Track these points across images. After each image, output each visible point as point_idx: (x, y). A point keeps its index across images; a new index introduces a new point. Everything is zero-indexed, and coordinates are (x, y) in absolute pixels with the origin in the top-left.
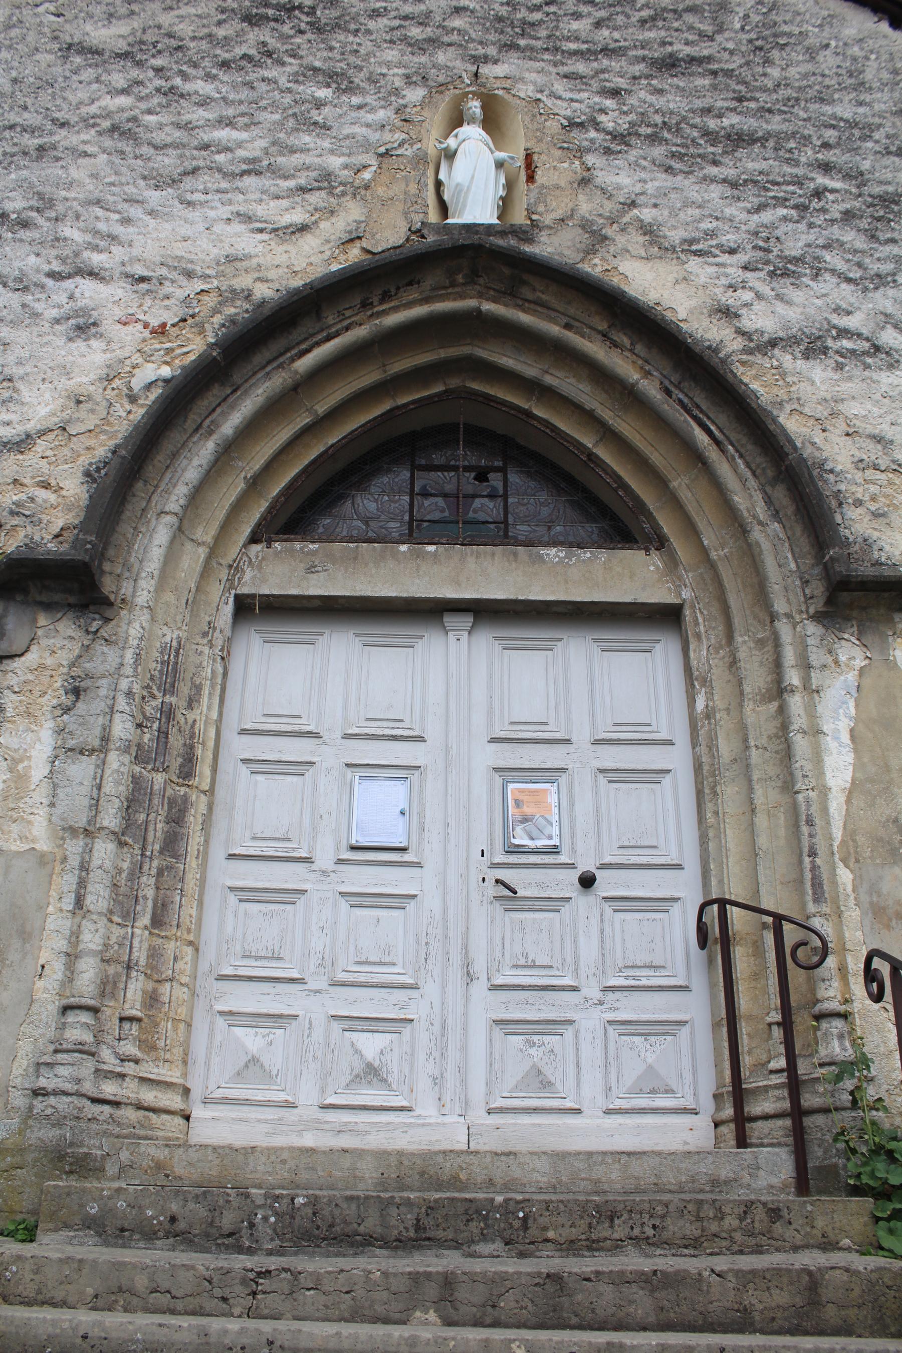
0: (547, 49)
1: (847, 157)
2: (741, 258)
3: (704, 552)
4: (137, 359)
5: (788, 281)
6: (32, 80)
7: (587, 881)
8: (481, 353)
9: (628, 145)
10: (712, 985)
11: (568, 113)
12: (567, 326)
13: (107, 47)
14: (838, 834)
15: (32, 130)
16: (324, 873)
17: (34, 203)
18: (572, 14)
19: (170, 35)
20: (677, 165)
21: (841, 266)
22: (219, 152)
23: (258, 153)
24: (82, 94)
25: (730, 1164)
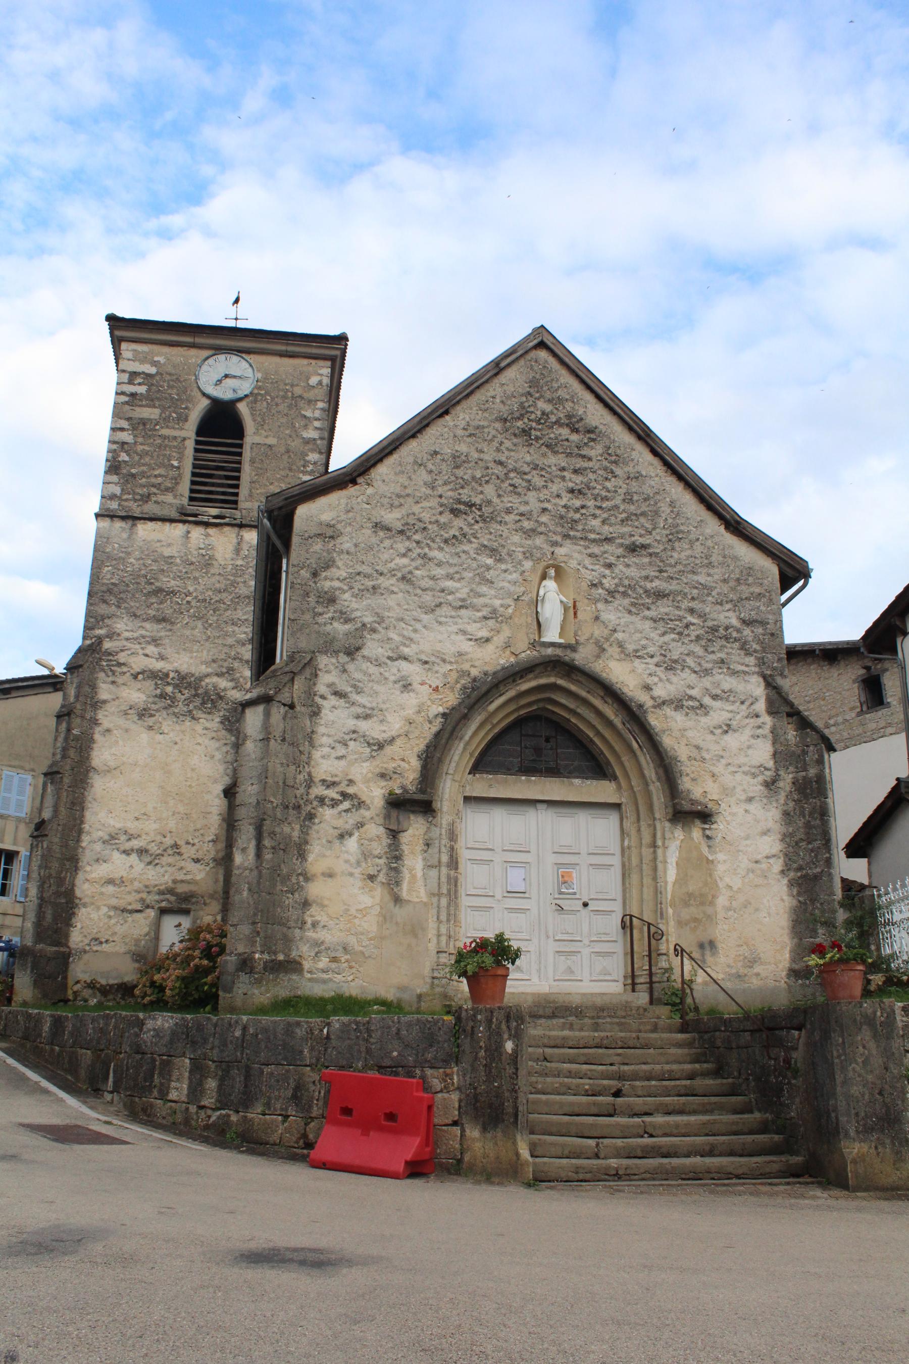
0: (582, 538)
1: (700, 606)
2: (655, 660)
3: (632, 788)
4: (429, 703)
5: (672, 672)
7: (585, 905)
8: (554, 697)
9: (613, 597)
10: (625, 941)
11: (590, 577)
12: (588, 692)
13: (392, 525)
14: (669, 897)
15: (367, 576)
16: (499, 901)
17: (375, 619)
18: (593, 515)
19: (420, 520)
20: (633, 610)
21: (692, 665)
22: (449, 594)
23: (465, 596)
24: (385, 556)
25: (630, 997)
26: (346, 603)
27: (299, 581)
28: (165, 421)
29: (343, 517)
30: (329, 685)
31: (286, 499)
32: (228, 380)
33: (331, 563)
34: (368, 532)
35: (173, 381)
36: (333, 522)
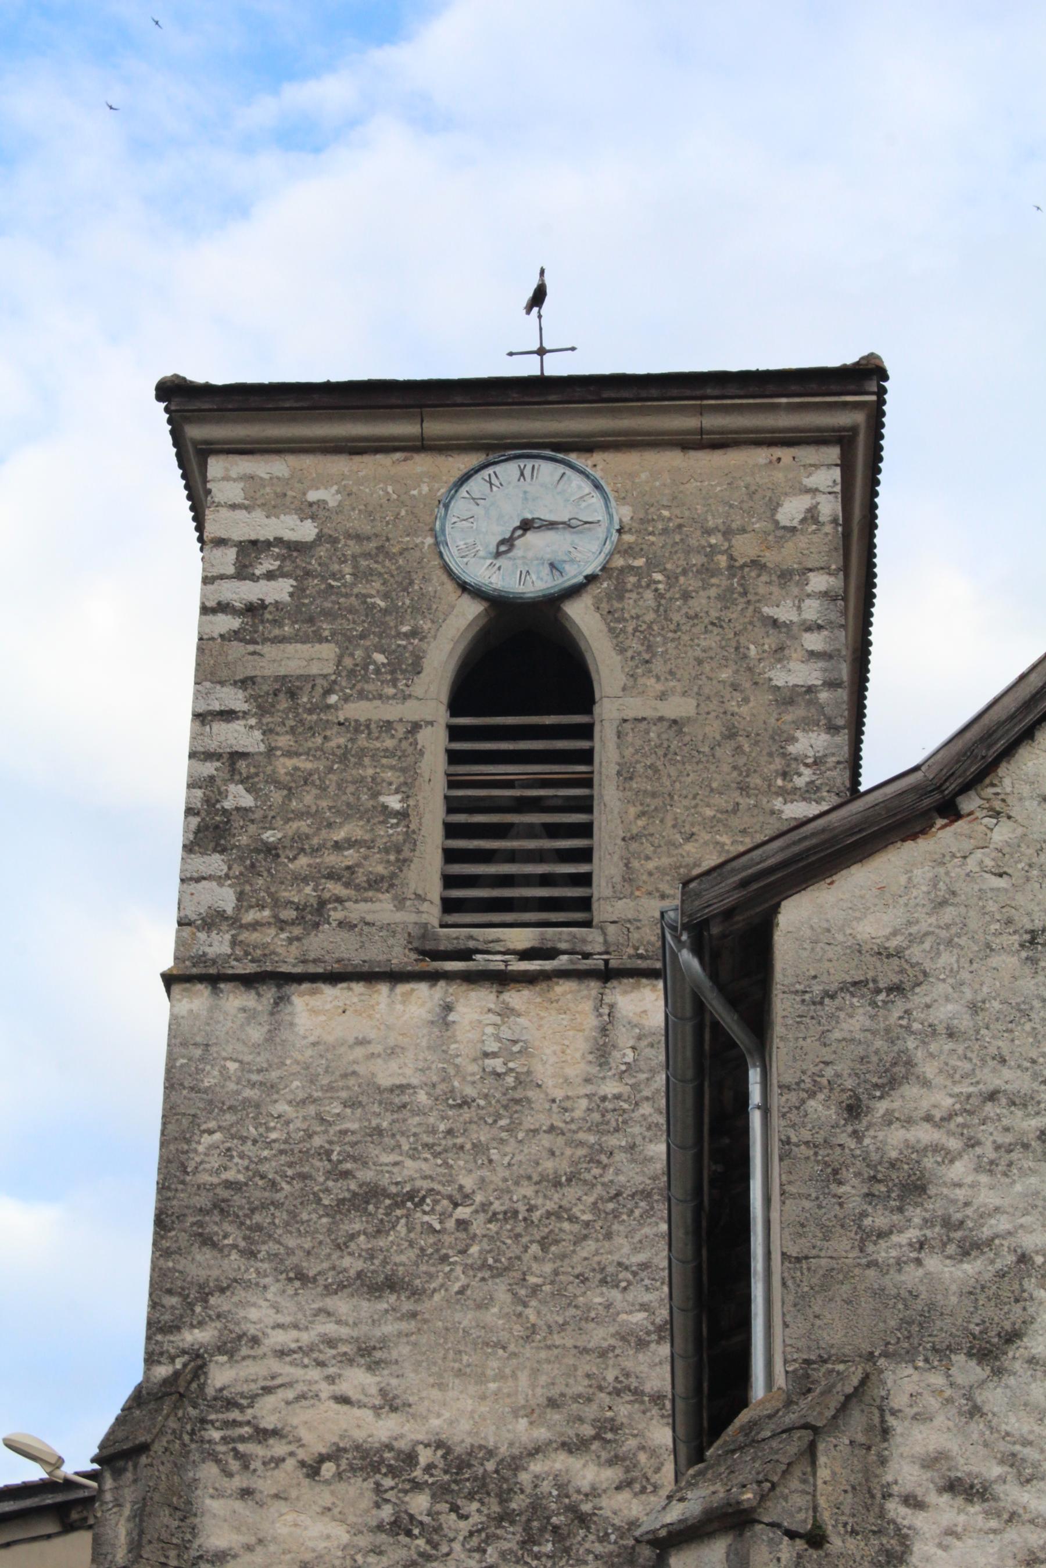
6: (996, 1005)
15: (1019, 1102)
26: (960, 1194)
27: (806, 1135)
28: (355, 677)
29: (926, 923)
30: (931, 1462)
31: (744, 883)
32: (530, 536)
33: (900, 1070)
34: (1008, 962)
35: (367, 555)
36: (893, 944)
